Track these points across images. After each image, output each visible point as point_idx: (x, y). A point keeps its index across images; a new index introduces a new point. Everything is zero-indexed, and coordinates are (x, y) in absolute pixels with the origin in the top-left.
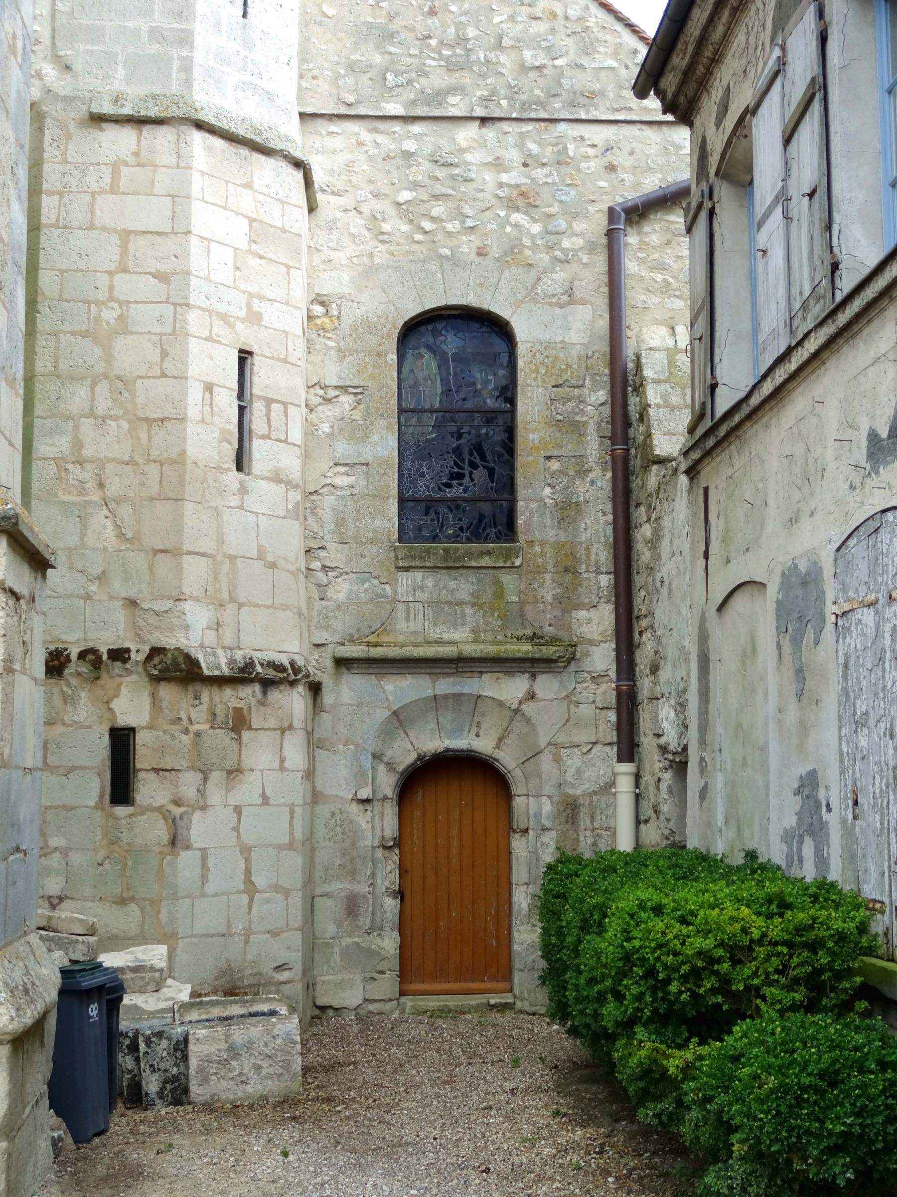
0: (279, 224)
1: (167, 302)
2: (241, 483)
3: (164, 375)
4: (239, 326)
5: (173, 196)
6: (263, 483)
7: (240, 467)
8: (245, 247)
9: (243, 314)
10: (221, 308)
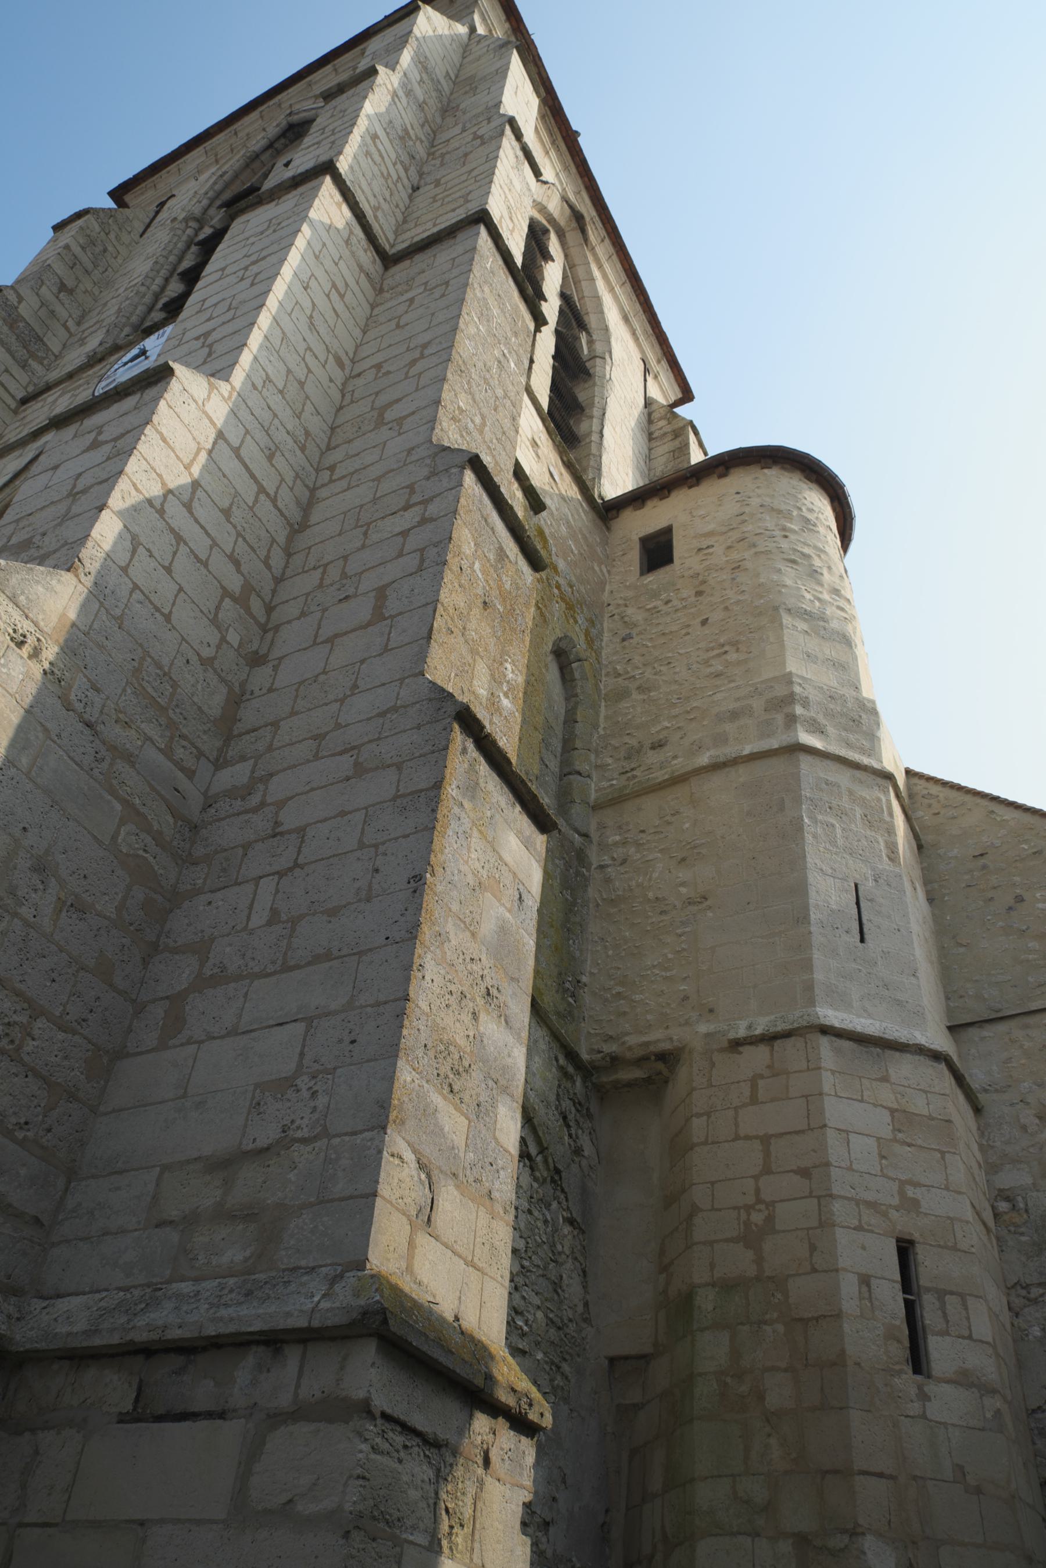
0: (925, 1112)
1: (810, 1196)
2: (920, 1388)
3: (814, 1270)
4: (894, 1214)
5: (806, 1096)
6: (946, 1388)
7: (917, 1369)
8: (890, 1136)
9: (896, 1201)
10: (870, 1196)
